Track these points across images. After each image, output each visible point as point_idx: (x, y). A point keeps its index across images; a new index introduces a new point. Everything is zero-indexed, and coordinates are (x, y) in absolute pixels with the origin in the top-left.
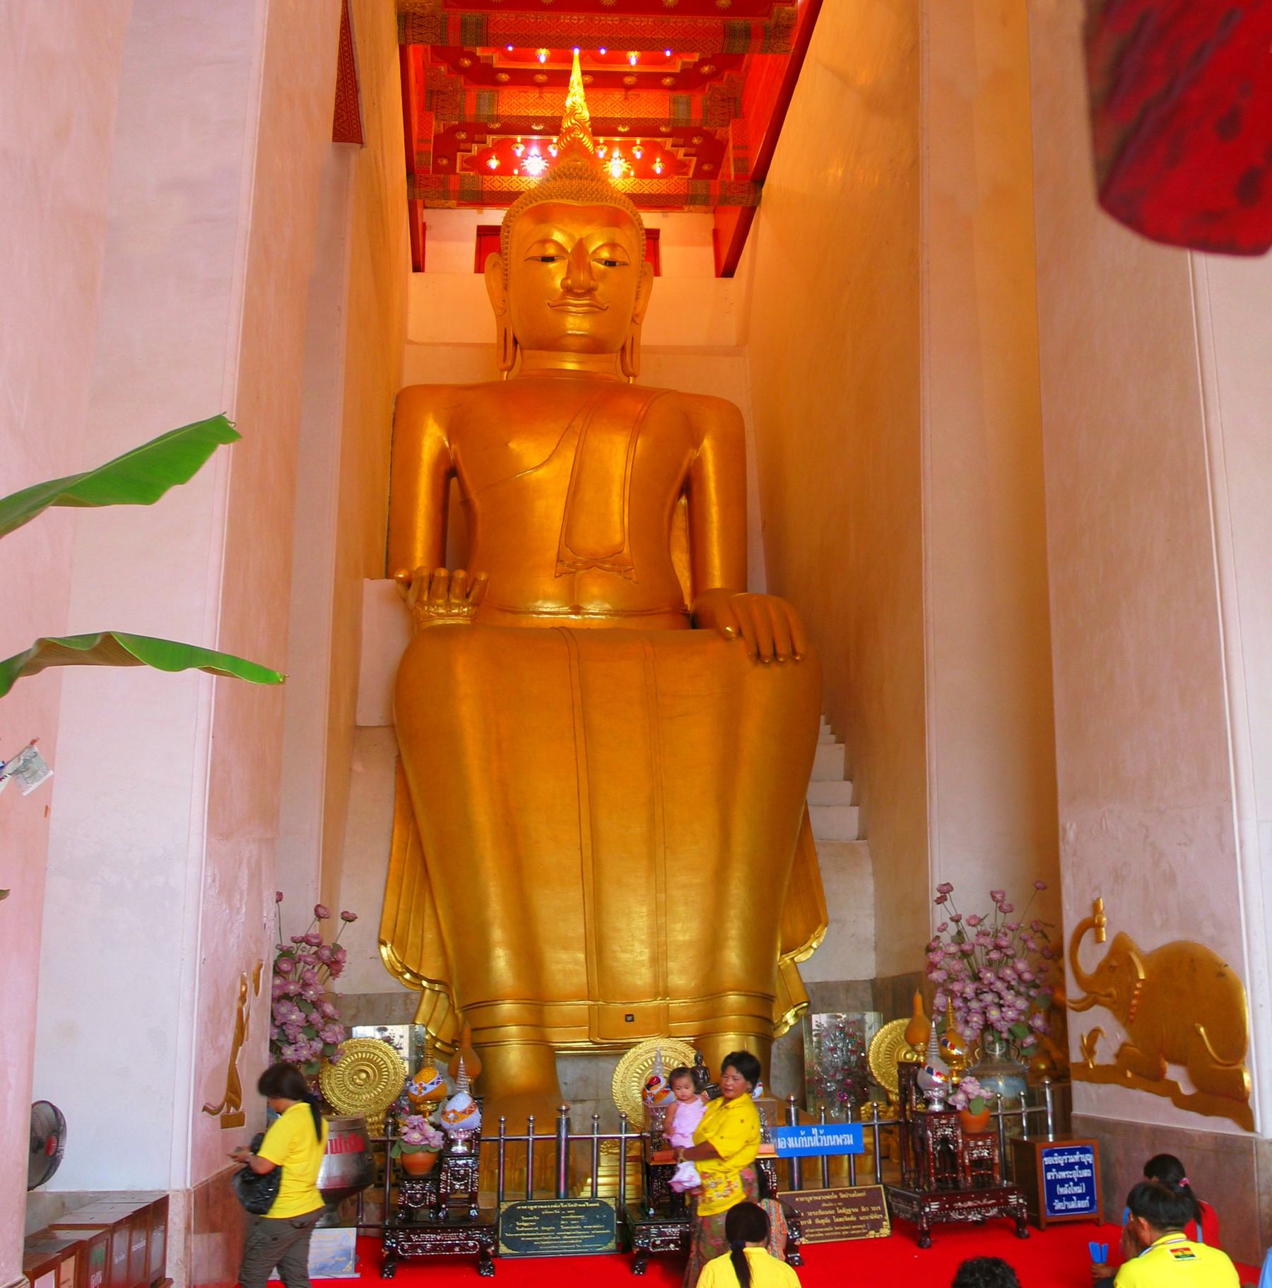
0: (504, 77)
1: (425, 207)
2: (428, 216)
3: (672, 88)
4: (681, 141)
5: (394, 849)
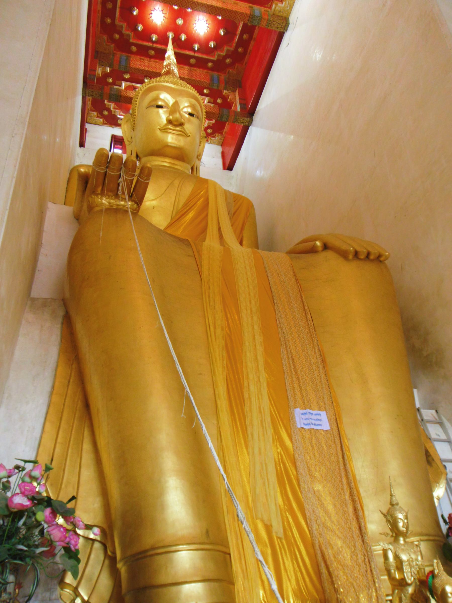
0: (134, 49)
1: (87, 123)
2: (87, 126)
3: (212, 69)
4: (212, 100)
5: (57, 384)
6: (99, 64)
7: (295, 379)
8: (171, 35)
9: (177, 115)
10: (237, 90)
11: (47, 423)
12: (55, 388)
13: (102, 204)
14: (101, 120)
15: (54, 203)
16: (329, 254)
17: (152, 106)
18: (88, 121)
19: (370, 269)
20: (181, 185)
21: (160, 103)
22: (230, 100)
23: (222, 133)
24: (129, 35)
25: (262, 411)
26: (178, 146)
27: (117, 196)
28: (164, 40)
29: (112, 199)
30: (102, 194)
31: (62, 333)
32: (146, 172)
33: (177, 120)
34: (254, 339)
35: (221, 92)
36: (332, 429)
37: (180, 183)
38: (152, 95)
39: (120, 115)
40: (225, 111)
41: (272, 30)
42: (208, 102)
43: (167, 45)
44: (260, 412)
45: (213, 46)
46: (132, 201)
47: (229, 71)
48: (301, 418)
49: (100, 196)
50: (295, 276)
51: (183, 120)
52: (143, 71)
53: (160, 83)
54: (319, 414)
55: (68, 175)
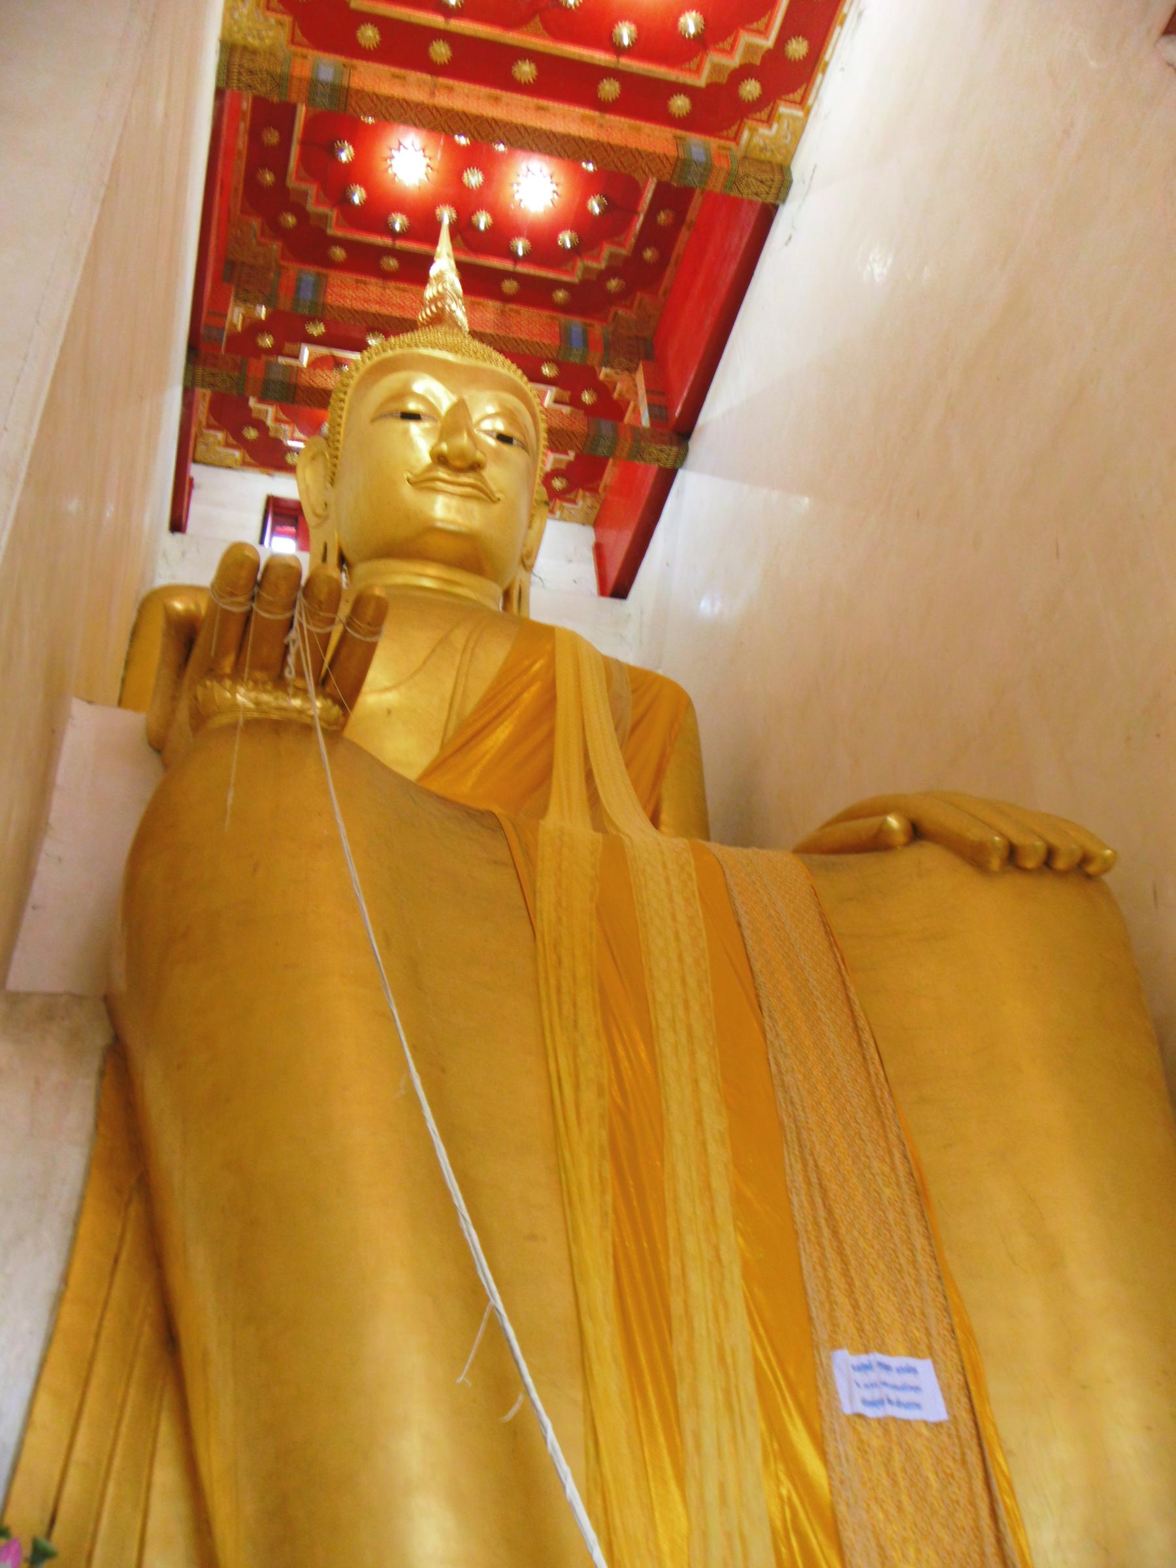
0: (339, 253)
1: (195, 461)
2: (195, 471)
4: (567, 395)
5: (77, 1266)
6: (237, 297)
7: (830, 1253)
8: (446, 215)
9: (464, 440)
10: (641, 367)
11: (43, 1399)
12: (72, 1282)
13: (235, 706)
14: (237, 454)
15: (90, 702)
16: (928, 855)
17: (391, 415)
18: (198, 456)
19: (1056, 900)
20: (471, 645)
21: (412, 406)
22: (620, 394)
23: (594, 491)
24: (324, 218)
25: (729, 1360)
26: (464, 529)
27: (280, 682)
28: (426, 229)
29: (265, 691)
30: (237, 675)
31: (98, 1106)
32: (370, 611)
33: (462, 455)
34: (700, 1122)
35: (593, 373)
36: (954, 1419)
37: (467, 641)
38: (391, 382)
39: (293, 439)
40: (606, 426)
41: (742, 200)
42: (556, 401)
43: (434, 242)
44: (722, 1360)
45: (569, 245)
46: (326, 696)
47: (616, 314)
48: (856, 1381)
49: (228, 683)
50: (825, 924)
51: (479, 455)
52: (365, 314)
53: (415, 350)
54: (912, 1370)
55: (133, 615)
